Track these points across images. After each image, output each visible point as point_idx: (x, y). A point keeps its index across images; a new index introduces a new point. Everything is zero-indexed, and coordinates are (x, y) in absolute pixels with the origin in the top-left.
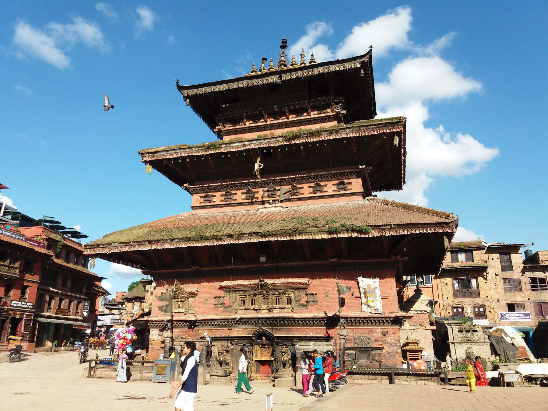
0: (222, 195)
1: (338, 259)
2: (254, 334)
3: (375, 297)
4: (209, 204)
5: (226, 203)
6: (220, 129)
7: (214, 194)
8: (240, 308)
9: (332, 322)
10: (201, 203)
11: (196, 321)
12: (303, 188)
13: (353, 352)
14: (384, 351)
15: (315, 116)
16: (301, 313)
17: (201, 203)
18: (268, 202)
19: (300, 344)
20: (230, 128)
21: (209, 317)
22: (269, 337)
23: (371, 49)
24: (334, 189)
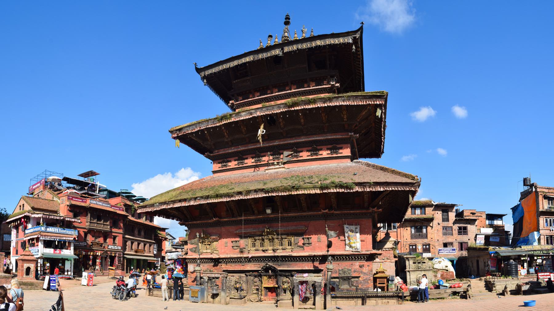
2: (262, 268)
3: (356, 240)
9: (323, 259)
11: (219, 259)
13: (338, 280)
14: (360, 279)
16: (298, 252)
18: (273, 164)
21: (229, 256)
22: (274, 270)
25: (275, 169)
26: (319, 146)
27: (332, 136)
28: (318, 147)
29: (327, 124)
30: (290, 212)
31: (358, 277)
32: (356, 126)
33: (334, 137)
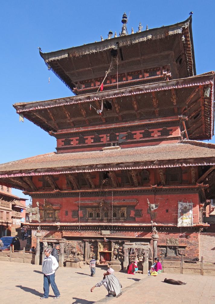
0: (77, 140)
1: (158, 185)
4: (68, 146)
5: (80, 145)
7: (71, 139)
8: (89, 218)
10: (62, 145)
12: (135, 134)
13: (165, 249)
14: (187, 248)
17: (62, 145)
18: (109, 145)
24: (158, 135)
26: (151, 129)
27: (162, 119)
28: (150, 130)
29: (158, 109)
30: (123, 187)
31: (184, 247)
32: (185, 110)
33: (165, 120)
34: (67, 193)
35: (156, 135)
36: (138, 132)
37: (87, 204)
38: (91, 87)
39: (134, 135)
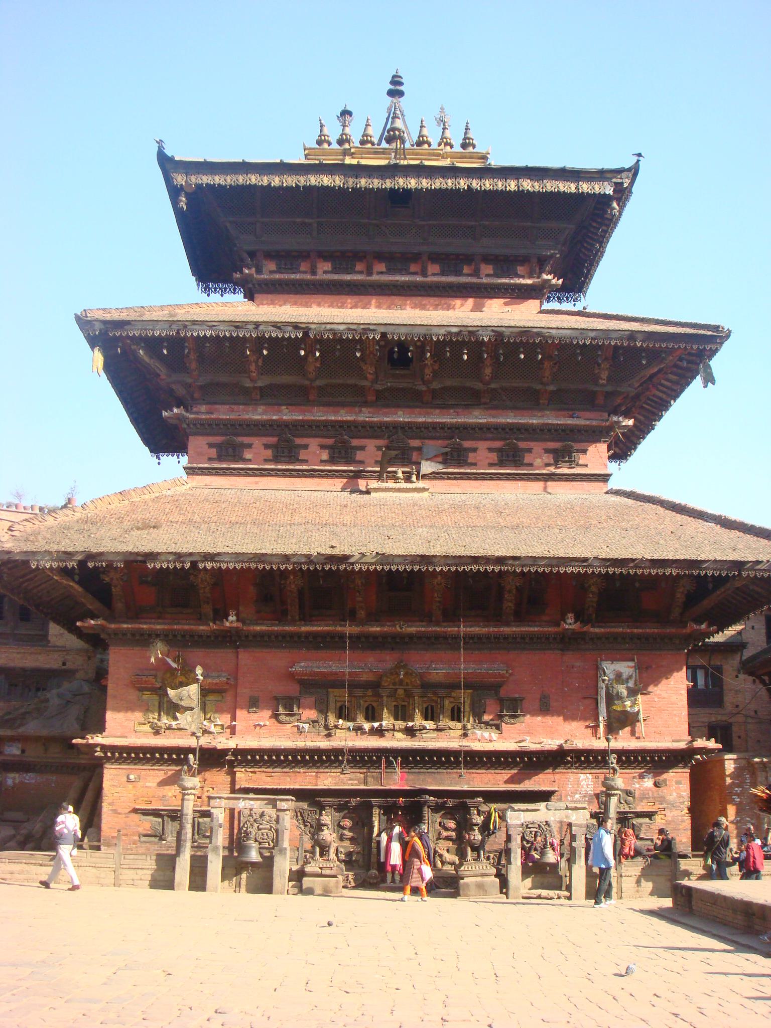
0: (267, 446)
6: (251, 275)
7: (246, 440)
11: (237, 752)
12: (475, 450)
15: (485, 280)
19: (516, 806)
20: (277, 276)
21: (267, 743)
23: (638, 161)
24: (546, 461)
25: (399, 490)
28: (522, 445)
34: (262, 635)
35: (538, 462)
36: (482, 446)
37: (332, 674)
38: (296, 270)
39: (471, 455)
